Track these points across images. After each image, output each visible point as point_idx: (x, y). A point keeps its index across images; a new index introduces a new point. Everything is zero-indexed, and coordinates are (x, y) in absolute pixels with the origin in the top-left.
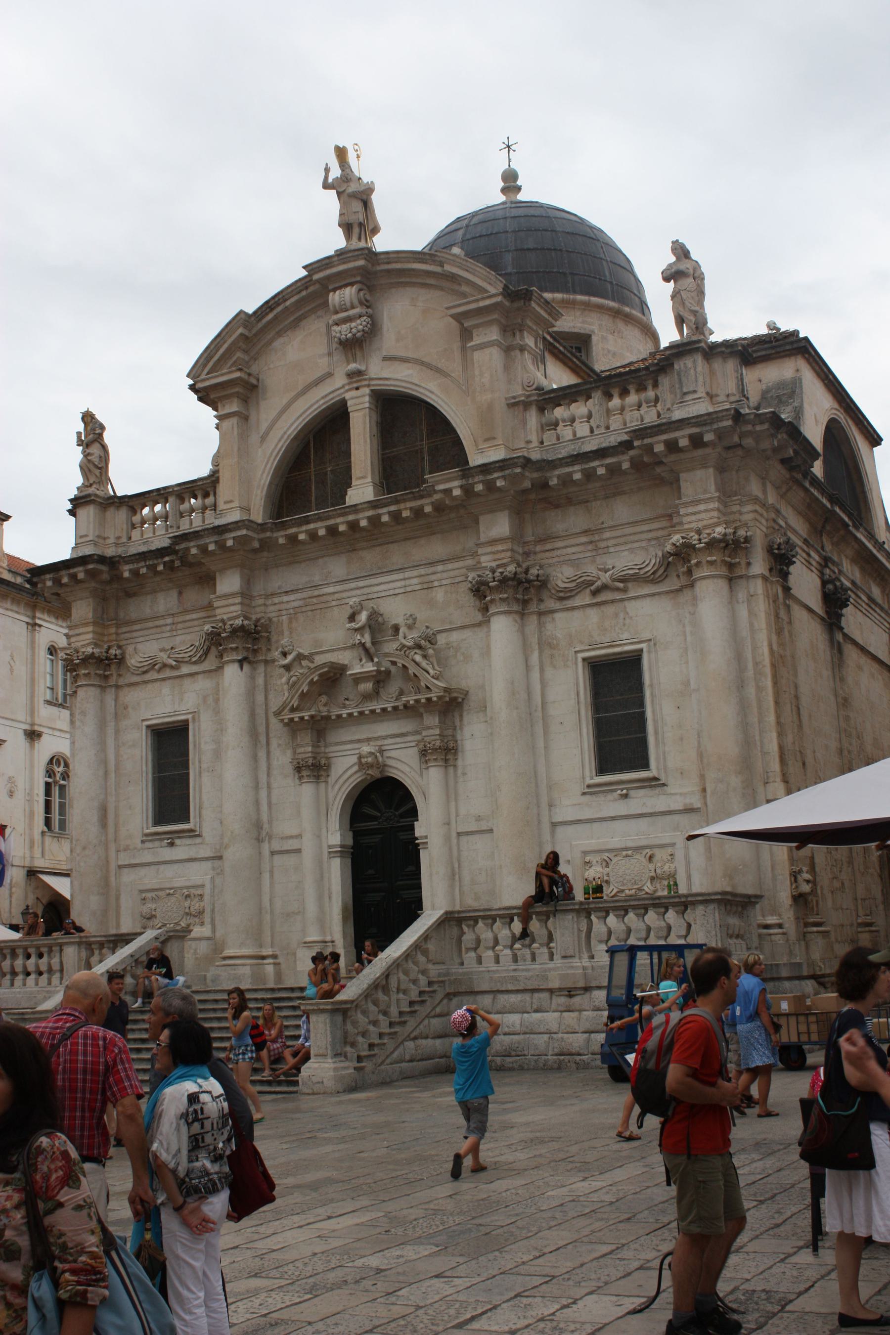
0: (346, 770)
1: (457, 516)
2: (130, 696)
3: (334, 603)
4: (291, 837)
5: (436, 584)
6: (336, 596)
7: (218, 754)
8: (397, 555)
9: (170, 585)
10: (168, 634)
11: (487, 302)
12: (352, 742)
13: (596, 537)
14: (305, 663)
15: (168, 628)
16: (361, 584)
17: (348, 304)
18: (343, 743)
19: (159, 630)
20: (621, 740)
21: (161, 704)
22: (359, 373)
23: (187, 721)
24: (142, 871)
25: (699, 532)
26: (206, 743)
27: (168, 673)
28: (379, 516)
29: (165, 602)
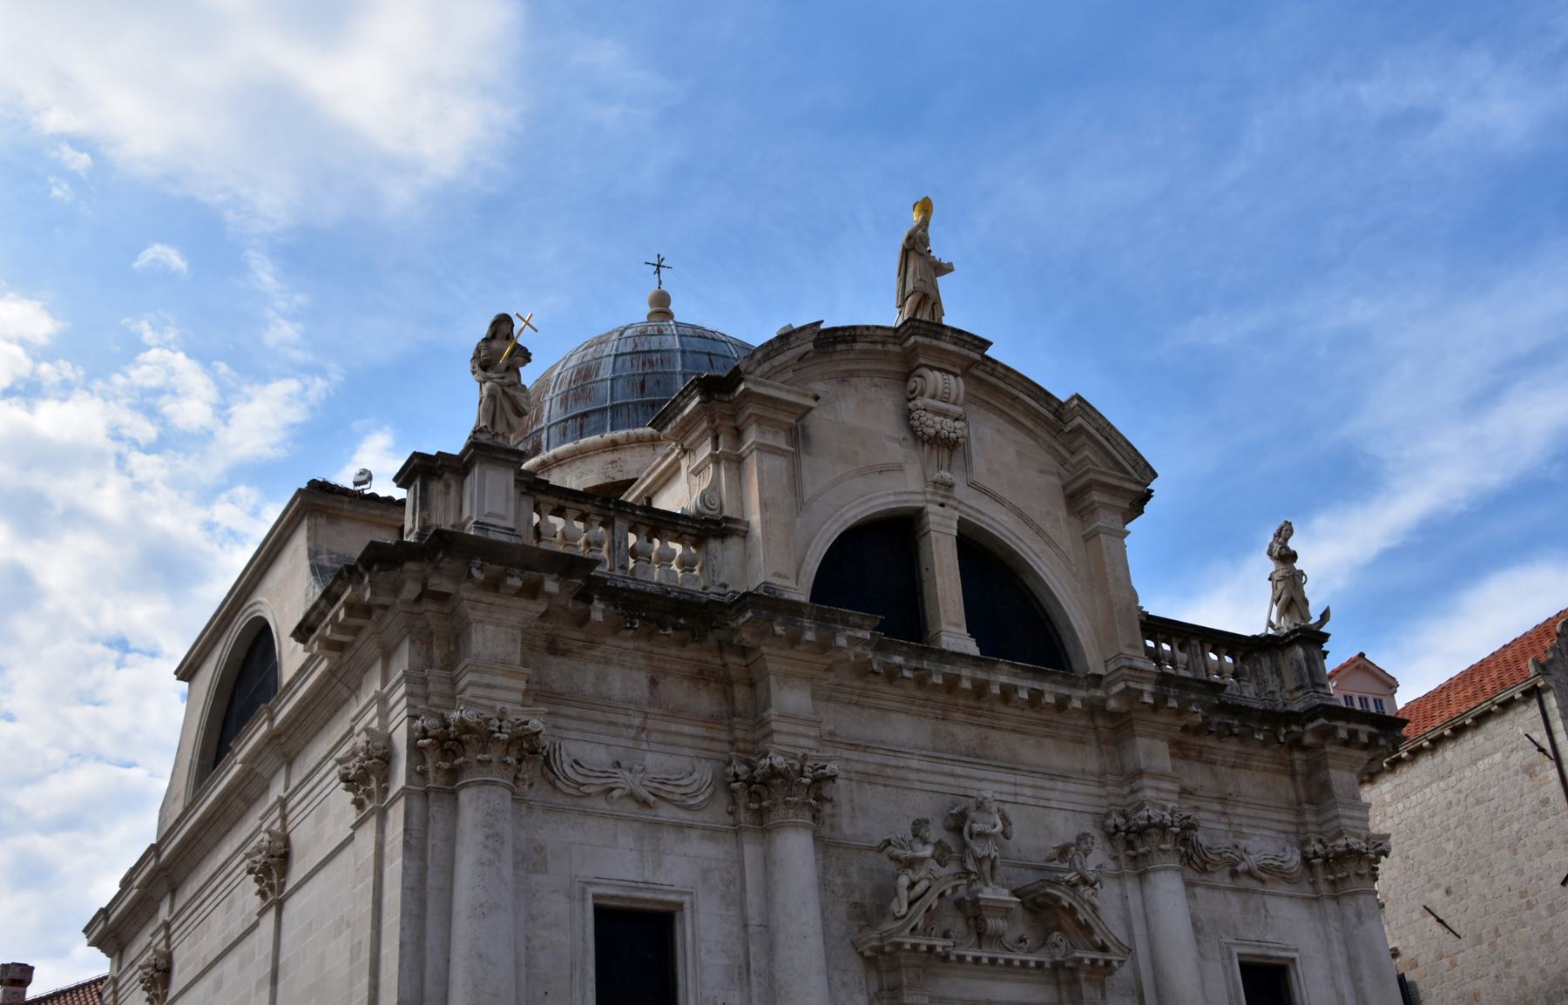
2: (556, 833)
3: (917, 785)
5: (1054, 804)
6: (923, 776)
9: (642, 662)
10: (630, 744)
15: (632, 733)
16: (958, 770)
21: (623, 864)
22: (950, 486)
23: (680, 905)
26: (709, 951)
27: (630, 807)
28: (1016, 689)
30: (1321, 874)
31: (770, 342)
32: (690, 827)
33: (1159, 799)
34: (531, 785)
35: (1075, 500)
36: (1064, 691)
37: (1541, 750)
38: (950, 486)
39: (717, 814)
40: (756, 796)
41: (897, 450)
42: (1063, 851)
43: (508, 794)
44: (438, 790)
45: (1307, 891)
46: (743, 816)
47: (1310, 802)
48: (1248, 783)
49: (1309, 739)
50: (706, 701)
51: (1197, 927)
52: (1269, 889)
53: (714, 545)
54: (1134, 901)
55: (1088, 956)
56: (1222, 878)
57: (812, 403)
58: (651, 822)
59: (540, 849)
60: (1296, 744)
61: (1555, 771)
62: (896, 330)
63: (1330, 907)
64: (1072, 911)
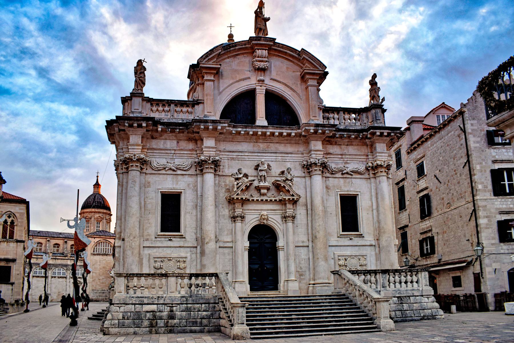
0: (252, 220)
1: (305, 139)
2: (151, 179)
4: (228, 242)
7: (199, 207)
8: (273, 147)
11: (319, 72)
12: (254, 210)
13: (344, 157)
14: (244, 178)
15: (172, 155)
16: (259, 154)
17: (264, 56)
18: (251, 210)
19: (167, 155)
20: (350, 221)
22: (263, 81)
23: (181, 192)
24: (155, 250)
25: (384, 162)
29: (170, 144)
30: (371, 172)
31: (207, 53)
32: (185, 175)
33: (317, 157)
34: (147, 169)
35: (303, 78)
36: (289, 131)
37: (461, 129)
38: (263, 81)
39: (192, 171)
40: (201, 166)
41: (248, 74)
42: (283, 173)
43: (138, 173)
44: (125, 172)
45: (367, 176)
46: (198, 172)
47: (372, 152)
48: (352, 150)
49: (369, 136)
50: (191, 146)
51: (327, 188)
52: (354, 176)
53: (196, 107)
54: (308, 182)
55: (287, 198)
56: (339, 175)
57: (219, 66)
58: (176, 175)
59: (149, 183)
60: (366, 138)
61: (464, 137)
62: (248, 41)
63: (373, 180)
64: (284, 187)
